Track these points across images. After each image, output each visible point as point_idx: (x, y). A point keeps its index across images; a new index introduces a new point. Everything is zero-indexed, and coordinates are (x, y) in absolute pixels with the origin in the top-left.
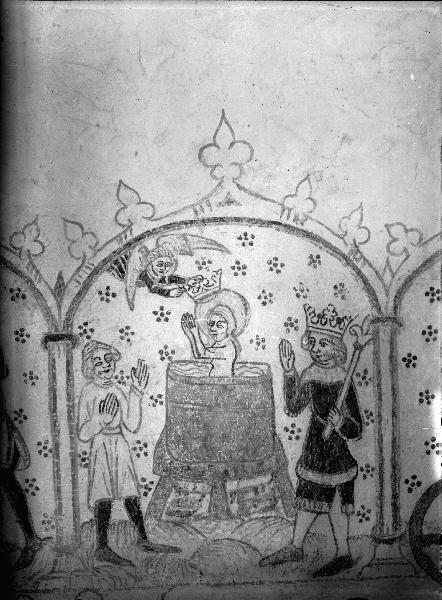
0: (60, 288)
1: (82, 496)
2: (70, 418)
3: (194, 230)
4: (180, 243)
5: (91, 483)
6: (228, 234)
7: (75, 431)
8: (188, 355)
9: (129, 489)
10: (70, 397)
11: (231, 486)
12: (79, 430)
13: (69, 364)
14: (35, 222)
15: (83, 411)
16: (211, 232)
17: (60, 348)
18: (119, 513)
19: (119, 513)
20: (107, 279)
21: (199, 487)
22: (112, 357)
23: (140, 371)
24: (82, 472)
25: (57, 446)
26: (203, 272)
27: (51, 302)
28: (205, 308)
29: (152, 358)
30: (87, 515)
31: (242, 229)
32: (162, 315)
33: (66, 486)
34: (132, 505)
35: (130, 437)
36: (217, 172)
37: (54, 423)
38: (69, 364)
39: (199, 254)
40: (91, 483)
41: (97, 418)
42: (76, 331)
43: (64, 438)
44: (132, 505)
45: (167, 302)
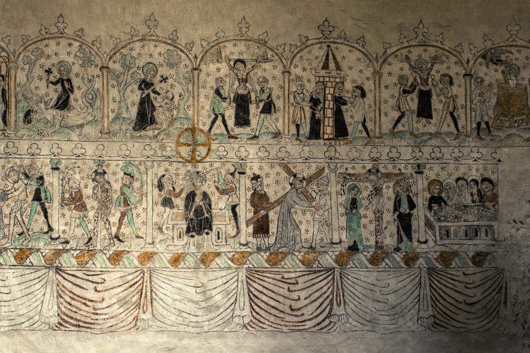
0: (468, 62)
1: (473, 119)
2: (470, 98)
3: (504, 48)
4: (500, 51)
5: (476, 116)
6: (513, 50)
7: (471, 101)
8: (503, 81)
9: (486, 119)
10: (470, 92)
11: (515, 119)
12: (473, 101)
13: (470, 82)
14: (461, 44)
15: (474, 96)
16: (509, 49)
17: (468, 78)
18: (483, 126)
19: (483, 126)
20: (480, 60)
21: (506, 119)
22: (482, 81)
23: (490, 85)
24: (473, 113)
25: (466, 106)
26: (508, 59)
27: (466, 65)
28: (508, 69)
29: (494, 82)
30: (474, 126)
31: (517, 49)
32: (496, 70)
33: (469, 117)
34: (487, 123)
35: (487, 104)
36: (511, 33)
37: (466, 99)
38: (470, 82)
39: (506, 54)
40: (476, 116)
41: (478, 98)
42: (472, 73)
43: (468, 103)
44: (487, 123)
45: (498, 67)
